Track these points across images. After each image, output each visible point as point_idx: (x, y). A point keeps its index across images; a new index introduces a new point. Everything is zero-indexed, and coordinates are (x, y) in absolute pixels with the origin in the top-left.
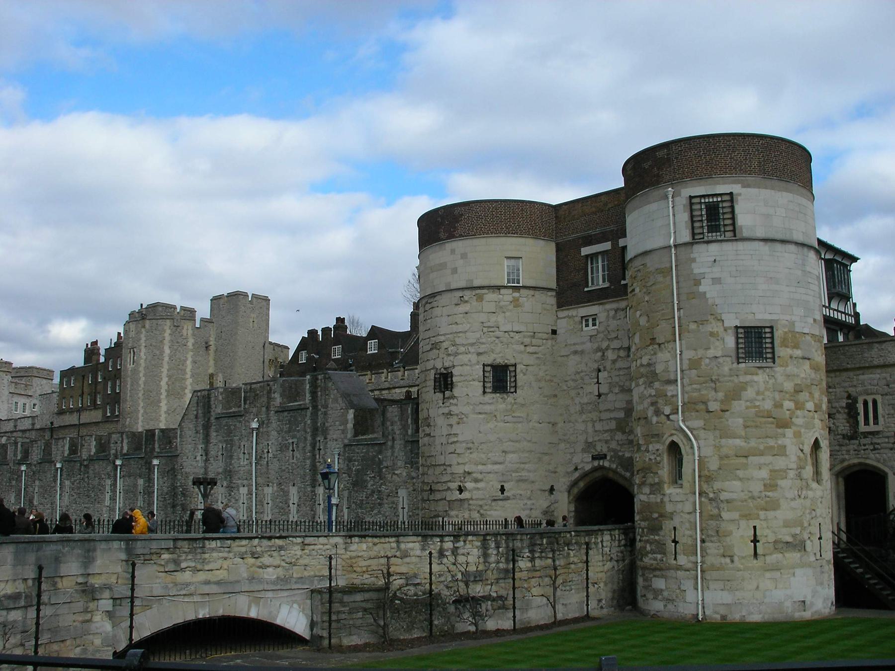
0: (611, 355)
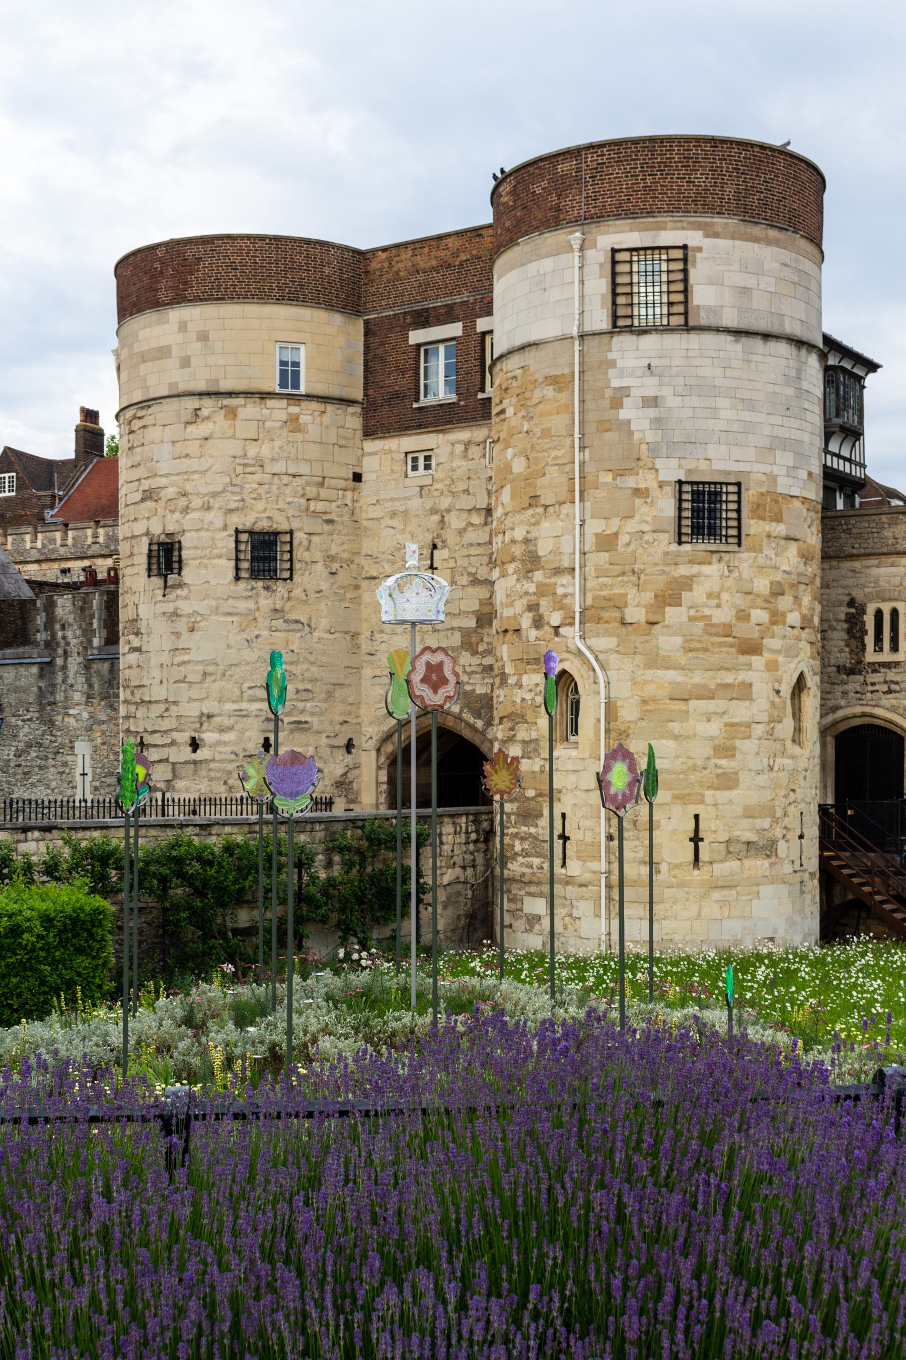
0: (455, 521)
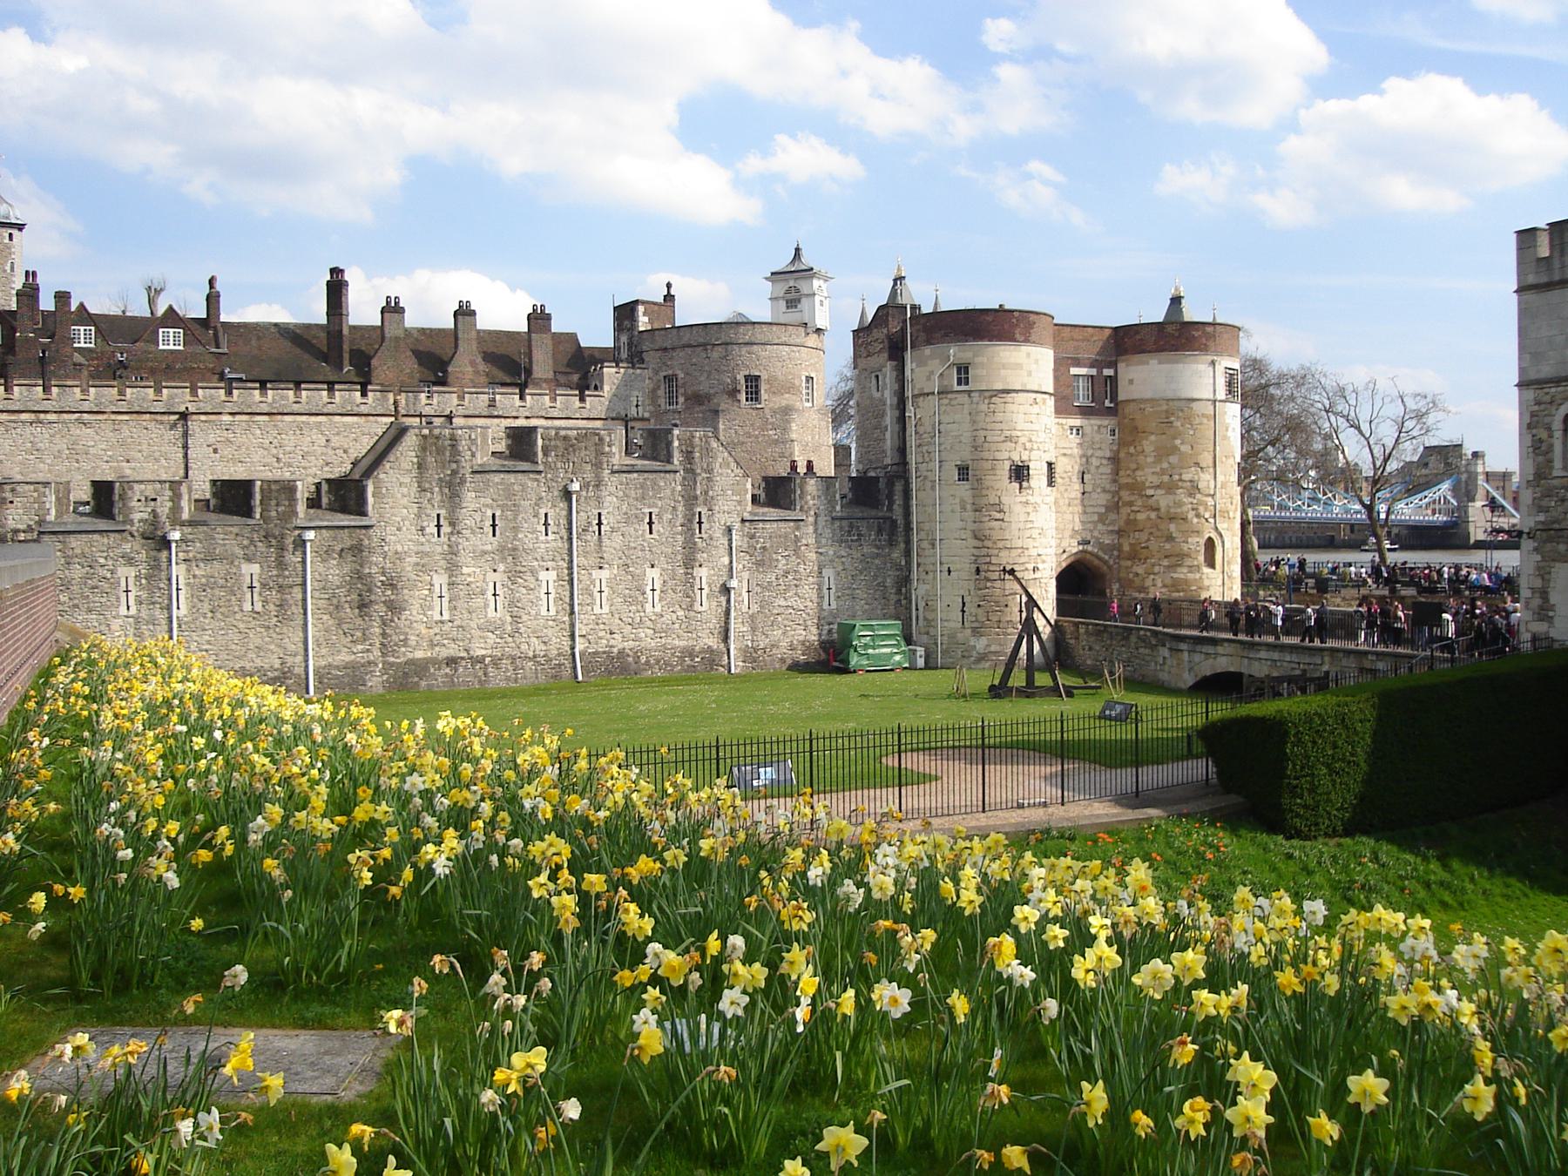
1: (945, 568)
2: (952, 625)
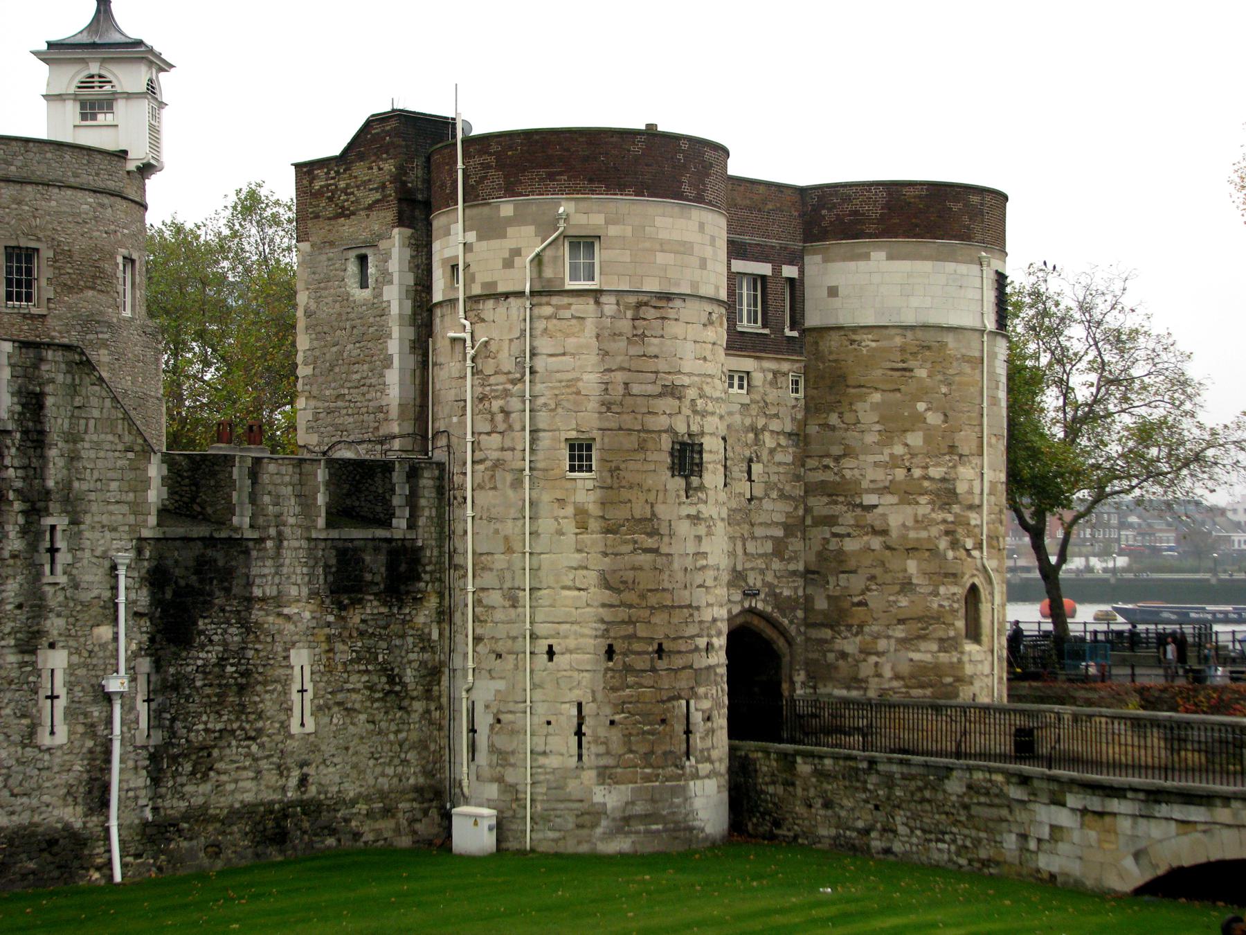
0: (769, 441)
1: (543, 645)
2: (552, 762)
